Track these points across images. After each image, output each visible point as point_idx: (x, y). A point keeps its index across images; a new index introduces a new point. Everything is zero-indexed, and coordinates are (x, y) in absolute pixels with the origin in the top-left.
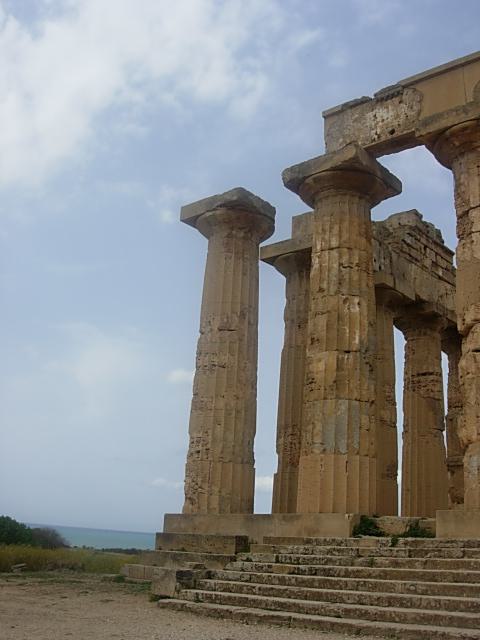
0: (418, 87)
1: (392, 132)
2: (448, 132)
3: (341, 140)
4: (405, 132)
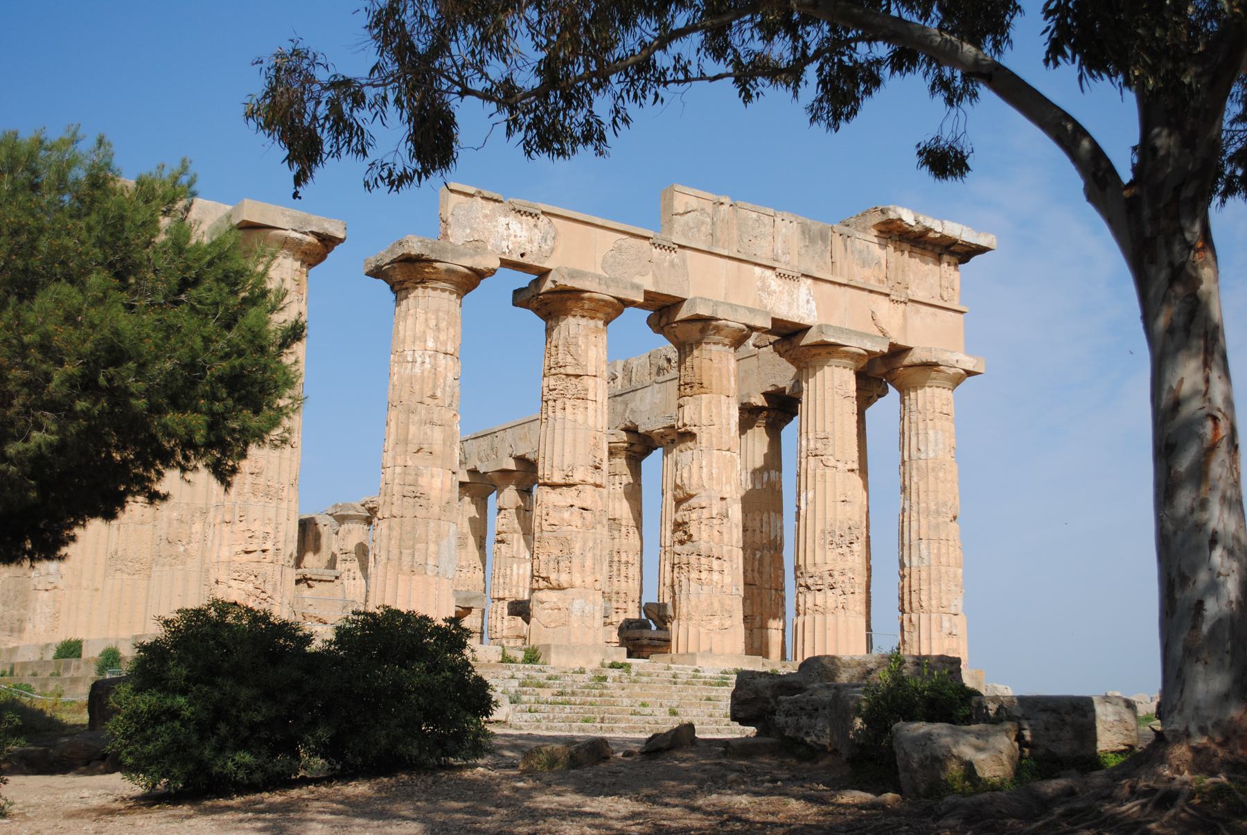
0: (554, 220)
2: (587, 295)
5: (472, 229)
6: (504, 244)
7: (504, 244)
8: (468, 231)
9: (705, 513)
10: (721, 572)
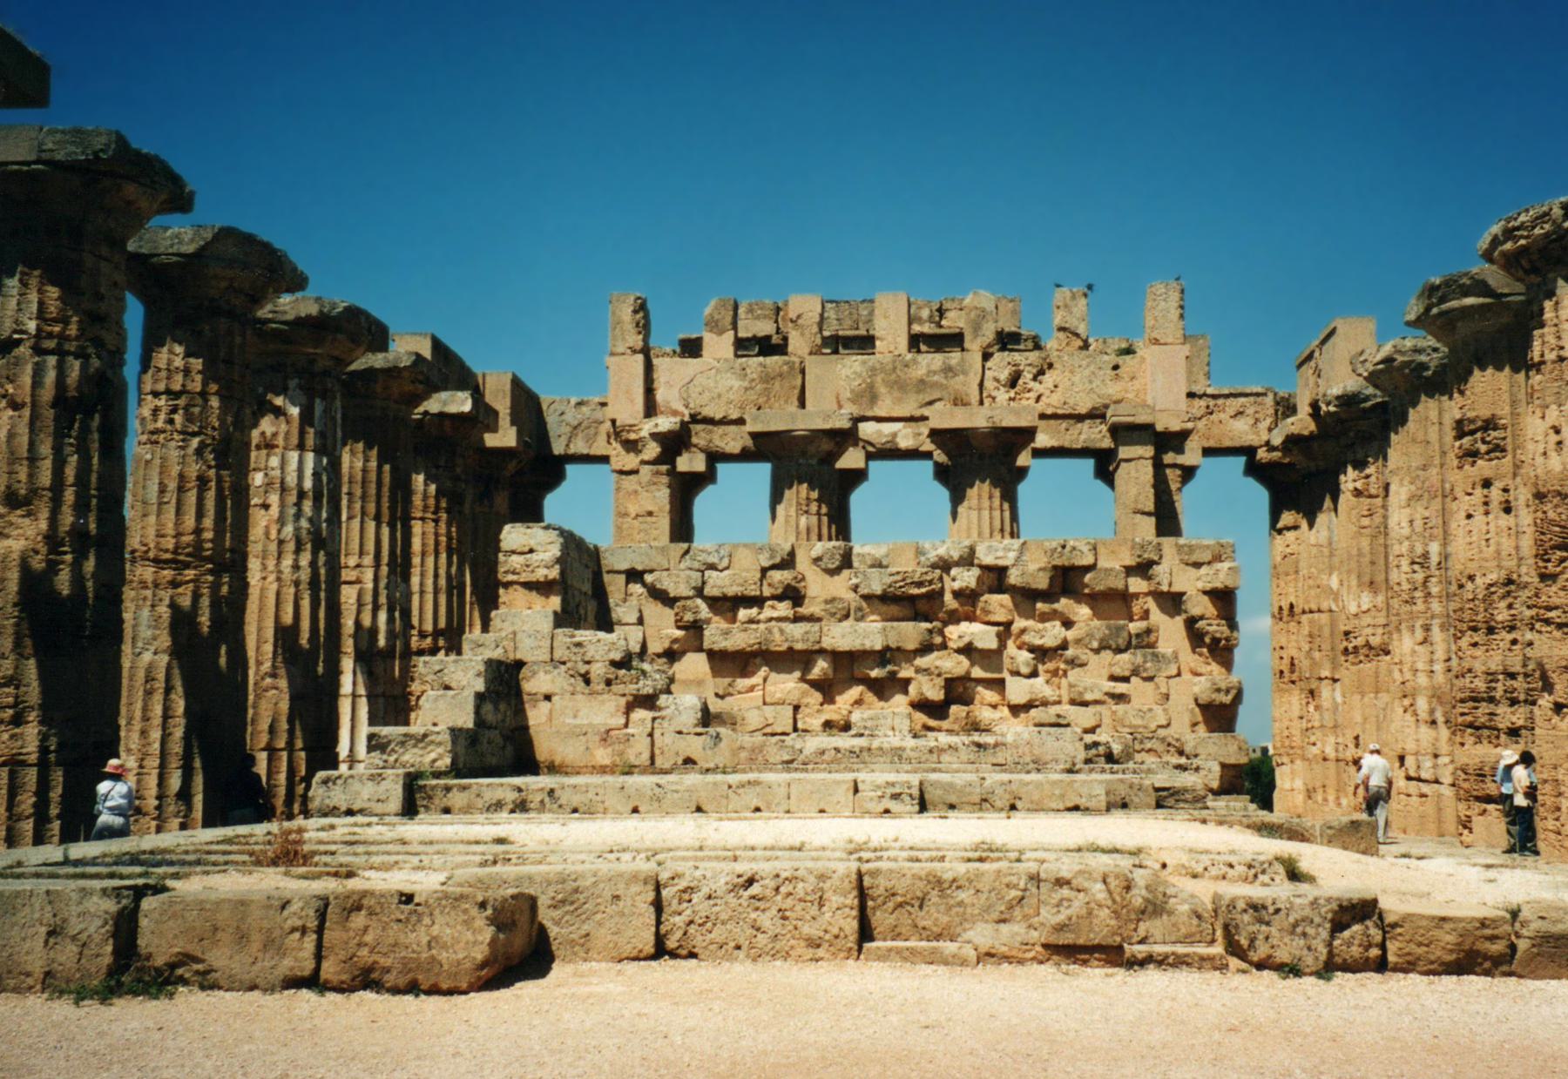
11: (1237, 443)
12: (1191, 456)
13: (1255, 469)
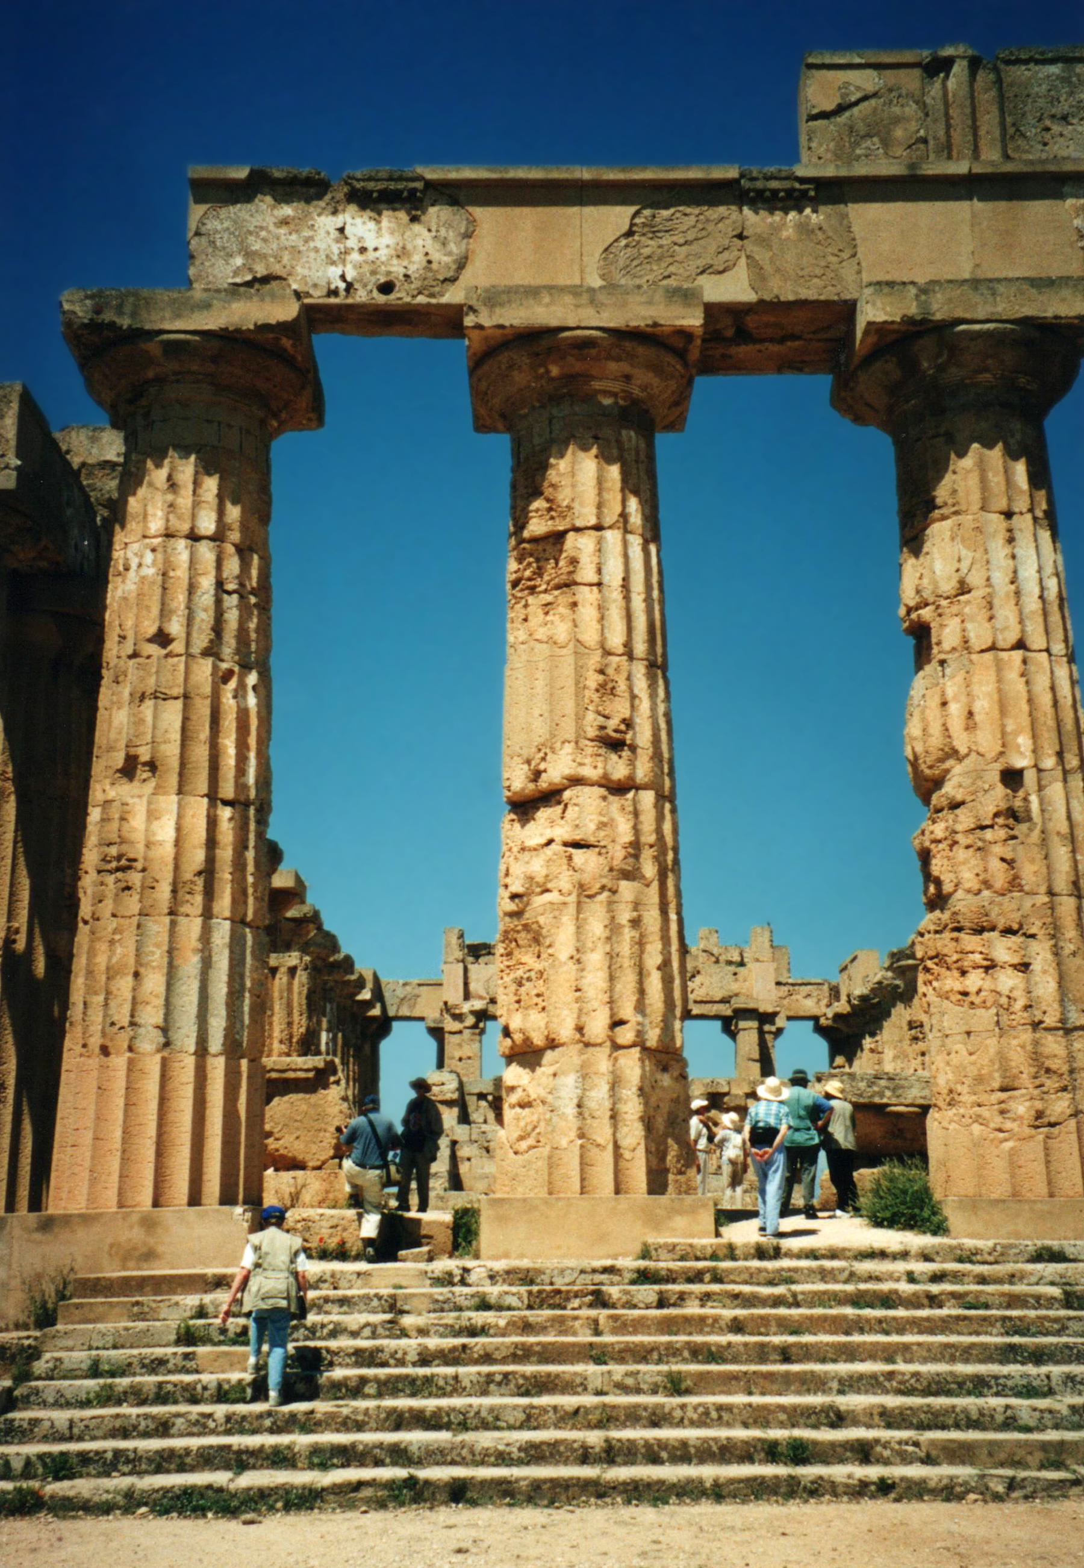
1: (386, 288)
3: (239, 261)
4: (421, 299)
5: (248, 254)
6: (335, 272)
7: (335, 272)
8: (239, 261)
9: (964, 819)
10: (1024, 967)
11: (808, 1014)
12: (780, 1022)
13: (819, 1029)
